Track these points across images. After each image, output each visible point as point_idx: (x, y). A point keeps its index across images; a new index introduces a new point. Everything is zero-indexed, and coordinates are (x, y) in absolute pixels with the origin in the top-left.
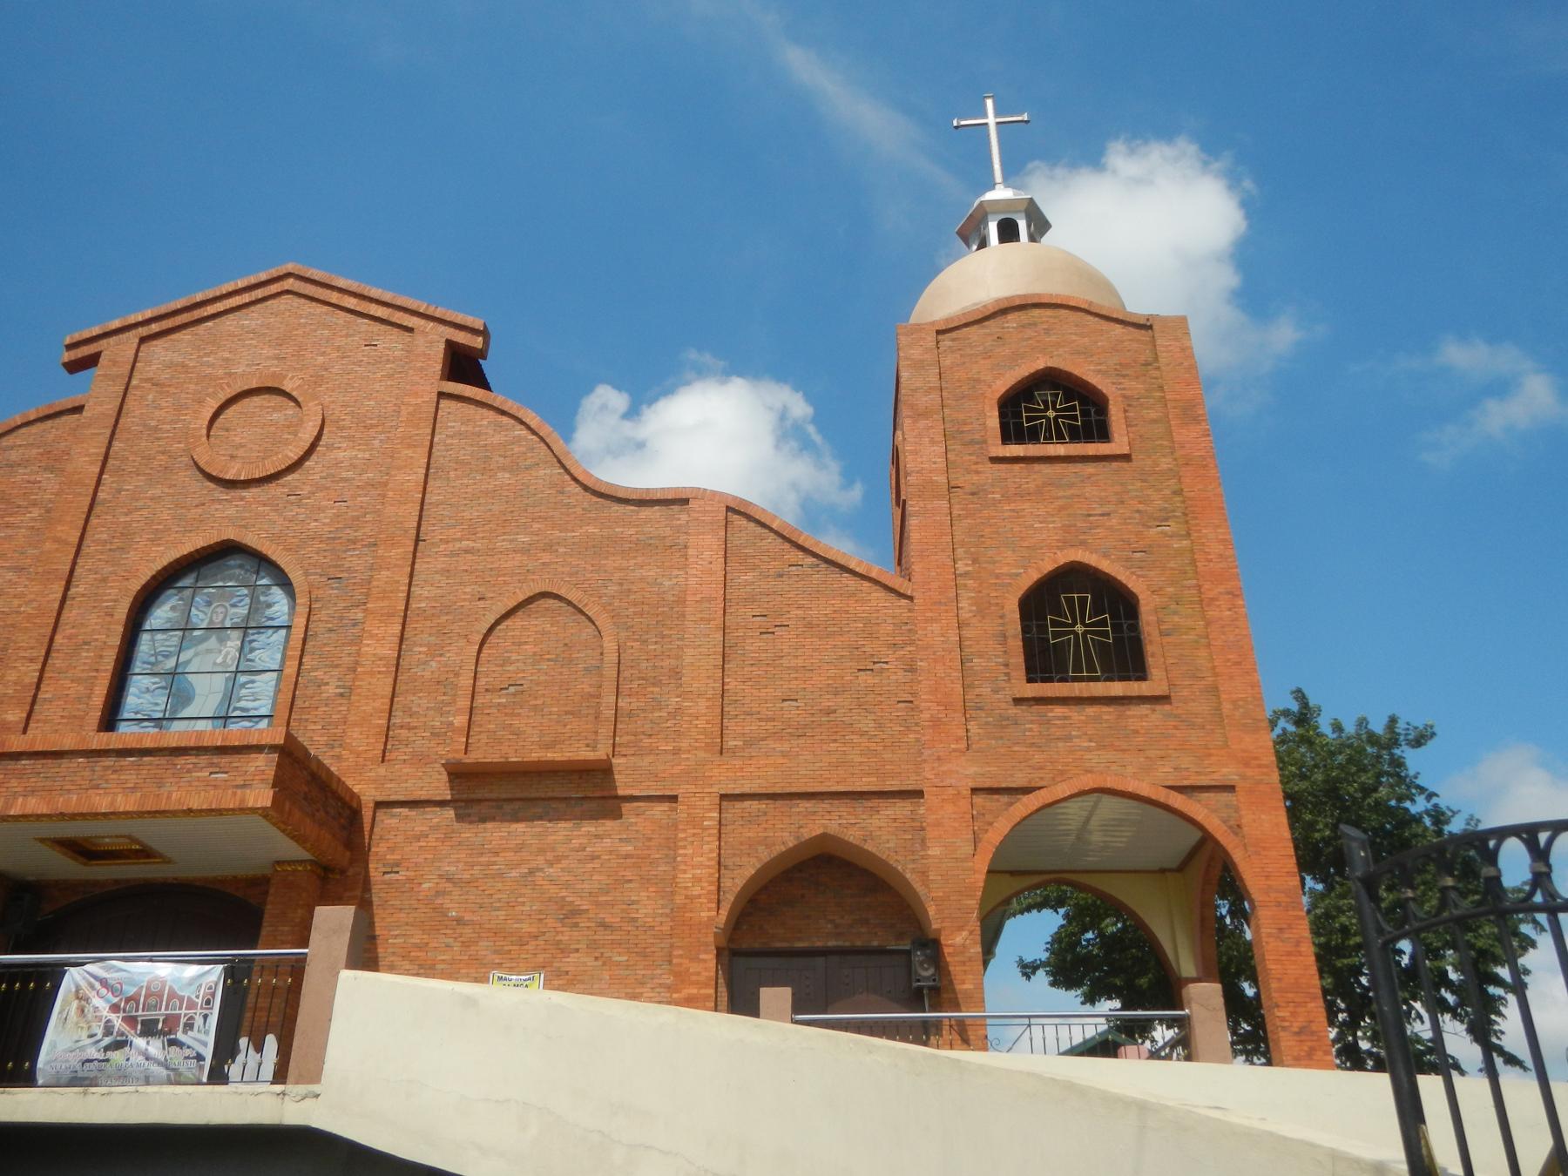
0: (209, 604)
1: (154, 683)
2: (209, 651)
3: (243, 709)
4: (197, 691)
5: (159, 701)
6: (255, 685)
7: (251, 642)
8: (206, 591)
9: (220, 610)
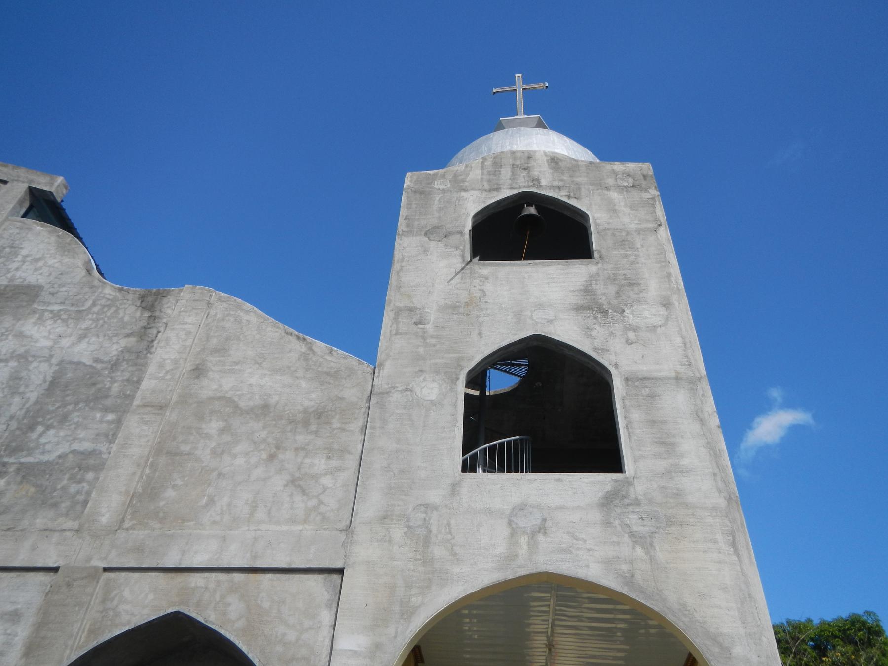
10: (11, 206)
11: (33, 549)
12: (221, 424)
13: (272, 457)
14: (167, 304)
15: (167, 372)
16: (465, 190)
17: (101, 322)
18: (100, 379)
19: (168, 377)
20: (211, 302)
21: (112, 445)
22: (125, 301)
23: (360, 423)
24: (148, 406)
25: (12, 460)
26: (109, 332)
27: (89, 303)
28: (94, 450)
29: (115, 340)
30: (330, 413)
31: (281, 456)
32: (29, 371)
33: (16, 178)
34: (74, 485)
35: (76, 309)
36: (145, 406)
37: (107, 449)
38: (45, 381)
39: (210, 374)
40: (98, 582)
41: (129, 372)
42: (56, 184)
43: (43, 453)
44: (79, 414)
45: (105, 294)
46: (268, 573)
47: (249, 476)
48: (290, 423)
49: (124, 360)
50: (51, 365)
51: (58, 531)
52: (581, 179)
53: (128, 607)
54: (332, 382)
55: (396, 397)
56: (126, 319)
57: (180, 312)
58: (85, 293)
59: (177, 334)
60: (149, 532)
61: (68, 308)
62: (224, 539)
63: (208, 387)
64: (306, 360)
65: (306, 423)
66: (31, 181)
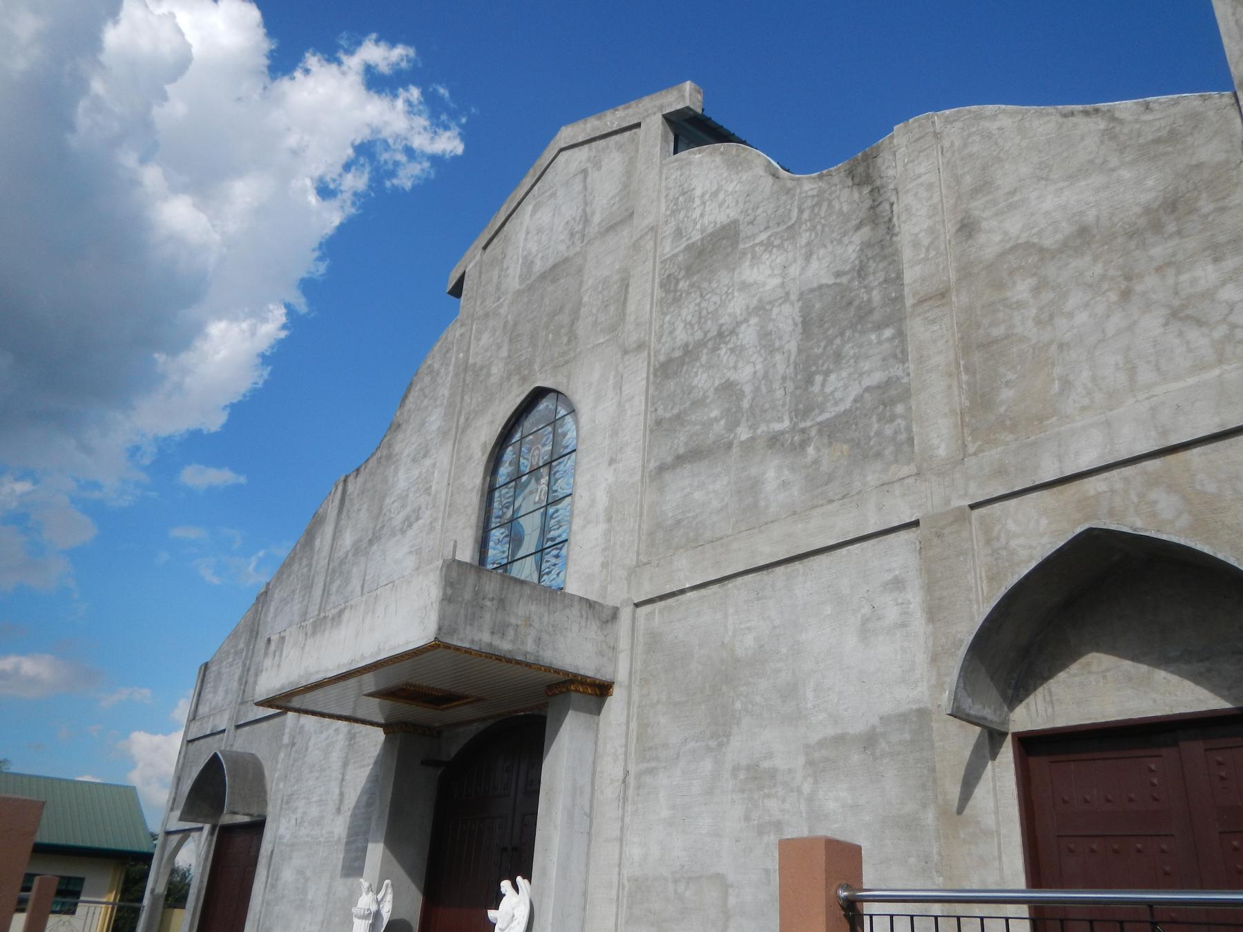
0: (529, 450)
1: (502, 534)
2: (531, 493)
3: (553, 539)
5: (505, 549)
6: (559, 513)
7: (555, 474)
8: (527, 439)
9: (536, 452)
10: (658, 148)
11: (880, 509)
12: (1031, 282)
13: (1126, 295)
14: (884, 164)
15: (928, 249)
17: (819, 227)
18: (853, 294)
19: (932, 254)
20: (938, 130)
21: (907, 365)
22: (833, 188)
24: (925, 300)
25: (808, 424)
26: (834, 235)
27: (795, 213)
28: (890, 379)
29: (846, 240)
30: (1188, 195)
31: (1139, 288)
32: (774, 320)
33: (646, 114)
34: (887, 426)
35: (785, 227)
36: (921, 302)
37: (904, 371)
38: (796, 325)
39: (984, 225)
40: (970, 523)
41: (881, 270)
42: (687, 94)
43: (836, 404)
44: (850, 345)
45: (806, 192)
46: (1195, 447)
47: (1103, 332)
48: (1131, 237)
49: (868, 259)
50: (792, 304)
51: (897, 481)
53: (1021, 541)
54: (1170, 149)
56: (845, 208)
57: (905, 165)
58: (784, 204)
59: (916, 195)
60: (1003, 448)
61: (775, 231)
62: (1108, 424)
63: (990, 243)
64: (1114, 137)
65: (1157, 227)
66: (661, 108)
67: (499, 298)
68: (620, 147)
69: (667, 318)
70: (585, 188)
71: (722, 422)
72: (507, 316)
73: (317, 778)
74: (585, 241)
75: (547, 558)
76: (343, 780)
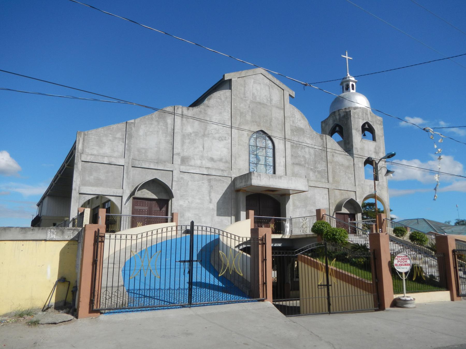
0: (259, 142)
2: (261, 152)
4: (261, 159)
9: (261, 143)
13: (345, 174)
16: (359, 119)
23: (353, 169)
36: (329, 162)
43: (319, 169)
52: (374, 120)
55: (357, 166)
56: (320, 141)
67: (245, 98)
68: (278, 90)
69: (292, 137)
70: (270, 91)
71: (304, 162)
72: (249, 105)
73: (196, 193)
74: (271, 105)
75: (267, 167)
76: (210, 196)
